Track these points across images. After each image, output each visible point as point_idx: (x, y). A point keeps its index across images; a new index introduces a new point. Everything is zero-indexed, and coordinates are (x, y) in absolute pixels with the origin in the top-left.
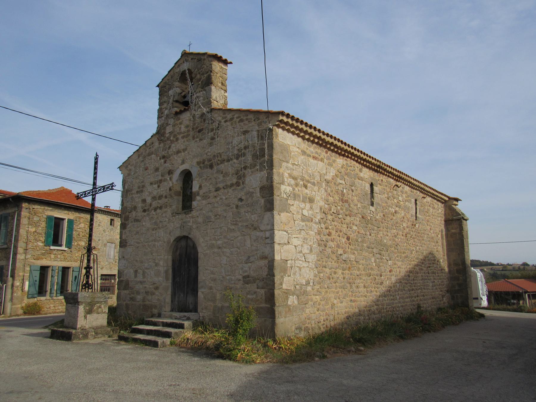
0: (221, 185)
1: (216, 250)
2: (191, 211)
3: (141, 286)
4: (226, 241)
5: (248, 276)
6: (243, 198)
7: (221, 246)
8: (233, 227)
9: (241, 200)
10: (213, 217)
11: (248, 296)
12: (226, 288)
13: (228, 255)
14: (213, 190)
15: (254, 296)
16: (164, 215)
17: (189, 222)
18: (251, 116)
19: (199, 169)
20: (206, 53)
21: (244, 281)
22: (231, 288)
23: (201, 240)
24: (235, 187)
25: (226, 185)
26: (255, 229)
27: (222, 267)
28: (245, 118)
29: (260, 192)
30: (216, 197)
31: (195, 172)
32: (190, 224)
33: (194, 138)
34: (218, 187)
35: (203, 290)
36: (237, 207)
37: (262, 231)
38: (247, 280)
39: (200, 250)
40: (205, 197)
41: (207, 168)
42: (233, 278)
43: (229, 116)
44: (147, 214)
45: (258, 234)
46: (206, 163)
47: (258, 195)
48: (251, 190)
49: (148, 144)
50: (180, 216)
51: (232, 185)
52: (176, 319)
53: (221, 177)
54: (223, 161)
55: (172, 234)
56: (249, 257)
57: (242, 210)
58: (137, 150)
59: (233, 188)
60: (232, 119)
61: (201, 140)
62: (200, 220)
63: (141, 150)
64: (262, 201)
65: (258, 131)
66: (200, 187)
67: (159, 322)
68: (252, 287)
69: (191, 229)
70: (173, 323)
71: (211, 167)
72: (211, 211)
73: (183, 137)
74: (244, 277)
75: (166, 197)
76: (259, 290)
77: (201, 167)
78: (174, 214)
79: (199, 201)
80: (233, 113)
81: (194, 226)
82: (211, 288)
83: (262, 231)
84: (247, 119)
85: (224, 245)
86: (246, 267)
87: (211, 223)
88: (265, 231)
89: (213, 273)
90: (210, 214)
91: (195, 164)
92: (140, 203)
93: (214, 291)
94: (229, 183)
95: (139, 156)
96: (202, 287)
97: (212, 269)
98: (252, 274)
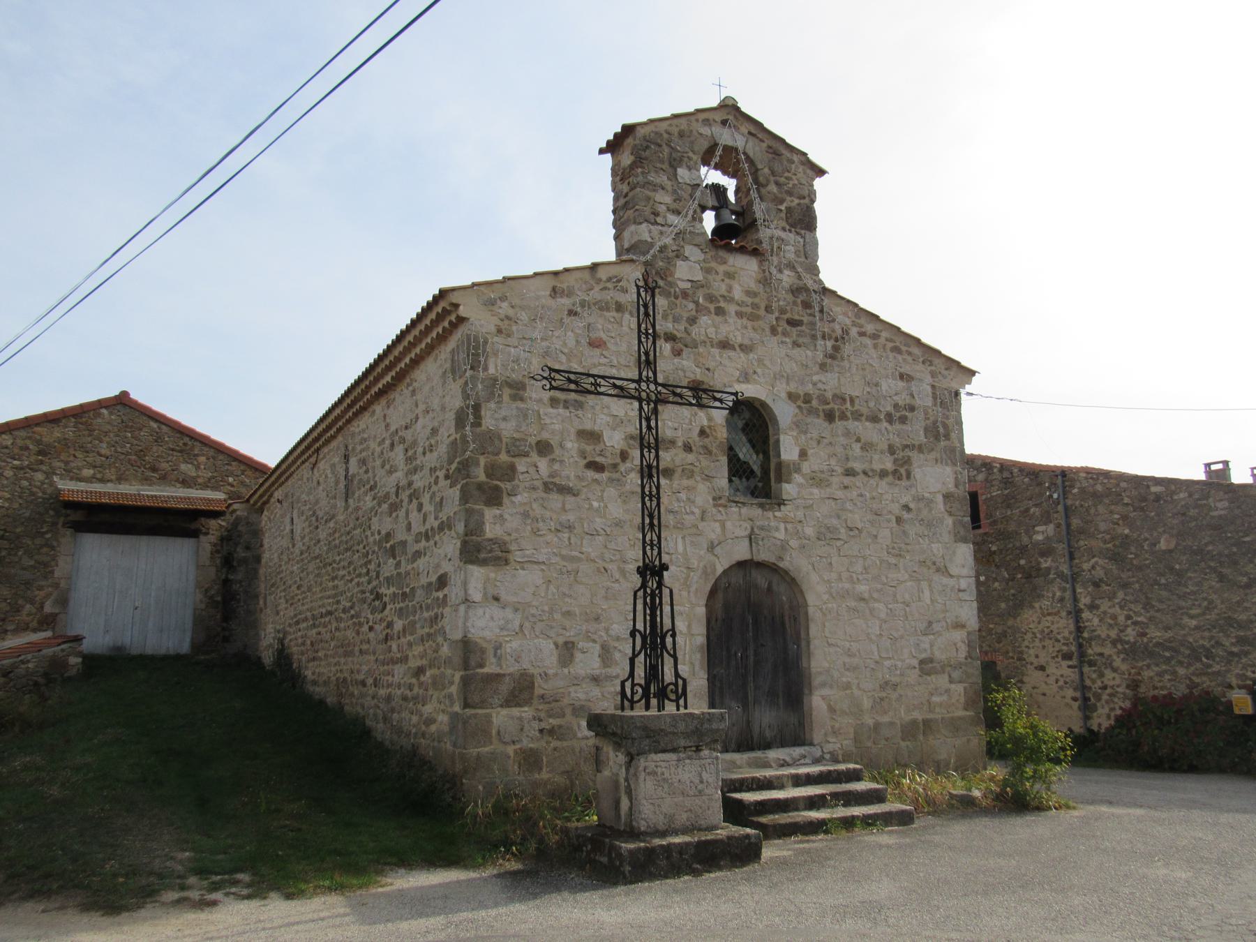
0: (858, 466)
1: (853, 604)
2: (779, 505)
3: (596, 692)
4: (879, 586)
5: (931, 660)
6: (912, 506)
7: (866, 596)
8: (893, 560)
9: (907, 508)
10: (843, 531)
11: (936, 699)
12: (885, 685)
13: (883, 615)
14: (839, 470)
15: (945, 698)
16: (683, 496)
17: (777, 529)
18: (916, 351)
19: (797, 411)
20: (805, 154)
21: (921, 670)
22: (895, 686)
23: (814, 578)
24: (890, 478)
25: (873, 470)
26: (938, 570)
27: (870, 639)
28: (904, 348)
29: (945, 504)
30: (846, 487)
31: (784, 412)
32: (781, 535)
33: (774, 331)
34: (852, 469)
35: (826, 691)
36: (899, 520)
37: (952, 576)
38: (927, 666)
39: (811, 599)
40: (817, 480)
41: (818, 416)
42: (899, 664)
43: (870, 328)
44: (611, 480)
45: (945, 580)
46: (815, 403)
47: (941, 506)
48: (927, 495)
49: (602, 274)
50: (744, 510)
51: (883, 474)
52: (782, 766)
53: (857, 447)
54: (857, 416)
55: (718, 550)
56: (930, 623)
57: (912, 531)
58: (556, 273)
59: (887, 480)
60: (875, 336)
61: (796, 344)
62: (809, 531)
63: (570, 280)
64: (949, 521)
65: (933, 387)
66: (803, 454)
67: (778, 777)
68: (942, 681)
69: (784, 546)
70: (830, 771)
71: (830, 417)
72: (839, 517)
73: (740, 315)
74: (922, 662)
75: (688, 448)
76: (953, 686)
77: (799, 407)
78: (722, 501)
79: (800, 485)
80: (879, 327)
81: (794, 543)
82: (848, 686)
83: (952, 576)
84: (910, 353)
85: (875, 595)
86: (926, 642)
87: (839, 543)
88: (959, 577)
89: (850, 654)
90: (835, 522)
91: (783, 395)
92: (573, 437)
93: (856, 692)
94: (877, 466)
95: (555, 292)
96: (823, 685)
97: (847, 645)
98: (938, 655)
